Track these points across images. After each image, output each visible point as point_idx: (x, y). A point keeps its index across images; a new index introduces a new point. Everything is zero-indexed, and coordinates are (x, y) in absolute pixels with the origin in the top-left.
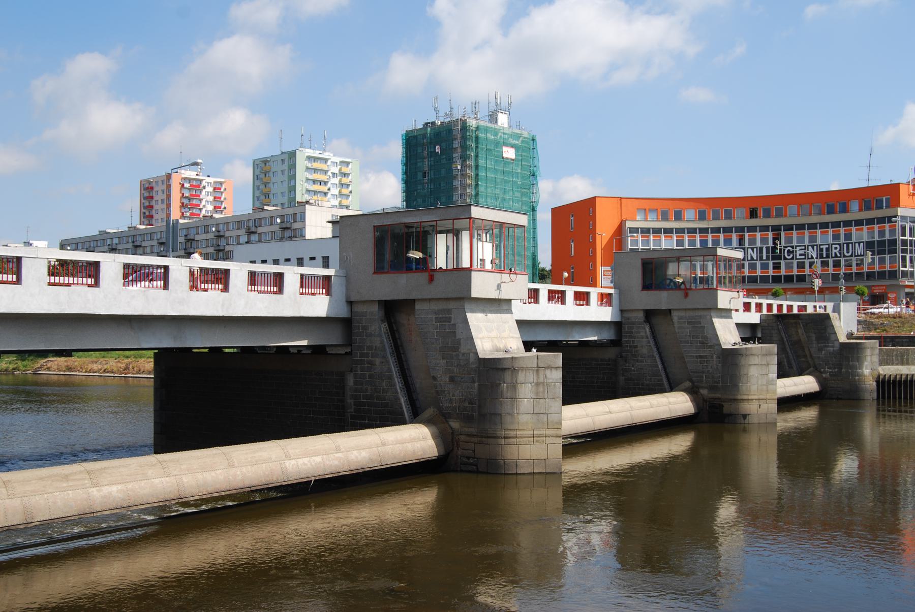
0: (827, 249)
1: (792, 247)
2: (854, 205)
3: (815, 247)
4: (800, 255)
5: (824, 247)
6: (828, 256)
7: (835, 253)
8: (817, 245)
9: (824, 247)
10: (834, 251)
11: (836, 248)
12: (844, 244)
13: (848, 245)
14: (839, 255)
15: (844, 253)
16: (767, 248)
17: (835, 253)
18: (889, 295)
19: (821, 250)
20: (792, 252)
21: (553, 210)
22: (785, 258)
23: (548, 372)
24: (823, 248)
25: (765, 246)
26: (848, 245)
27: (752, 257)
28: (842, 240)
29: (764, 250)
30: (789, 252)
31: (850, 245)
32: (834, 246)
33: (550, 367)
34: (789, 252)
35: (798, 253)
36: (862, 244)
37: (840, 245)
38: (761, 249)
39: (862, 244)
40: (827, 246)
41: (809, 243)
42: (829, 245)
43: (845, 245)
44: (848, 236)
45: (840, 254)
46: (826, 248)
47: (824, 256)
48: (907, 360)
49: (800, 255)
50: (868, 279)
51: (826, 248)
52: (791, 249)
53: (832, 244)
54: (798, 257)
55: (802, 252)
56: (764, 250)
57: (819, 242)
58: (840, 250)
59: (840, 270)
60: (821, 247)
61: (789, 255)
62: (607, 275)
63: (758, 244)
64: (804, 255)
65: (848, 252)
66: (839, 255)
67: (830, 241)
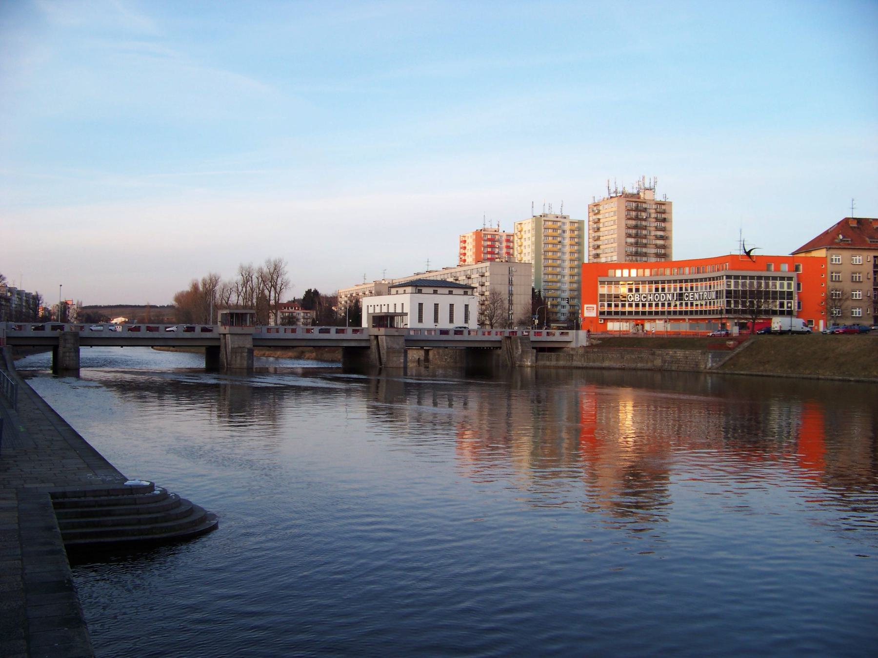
1: (688, 293)
2: (709, 268)
4: (692, 298)
5: (701, 293)
16: (677, 293)
19: (700, 295)
22: (685, 300)
23: (243, 354)
25: (675, 292)
27: (669, 299)
29: (675, 295)
33: (243, 352)
34: (687, 296)
35: (691, 296)
38: (673, 294)
48: (551, 359)
54: (691, 299)
55: (692, 296)
56: (675, 295)
63: (672, 291)
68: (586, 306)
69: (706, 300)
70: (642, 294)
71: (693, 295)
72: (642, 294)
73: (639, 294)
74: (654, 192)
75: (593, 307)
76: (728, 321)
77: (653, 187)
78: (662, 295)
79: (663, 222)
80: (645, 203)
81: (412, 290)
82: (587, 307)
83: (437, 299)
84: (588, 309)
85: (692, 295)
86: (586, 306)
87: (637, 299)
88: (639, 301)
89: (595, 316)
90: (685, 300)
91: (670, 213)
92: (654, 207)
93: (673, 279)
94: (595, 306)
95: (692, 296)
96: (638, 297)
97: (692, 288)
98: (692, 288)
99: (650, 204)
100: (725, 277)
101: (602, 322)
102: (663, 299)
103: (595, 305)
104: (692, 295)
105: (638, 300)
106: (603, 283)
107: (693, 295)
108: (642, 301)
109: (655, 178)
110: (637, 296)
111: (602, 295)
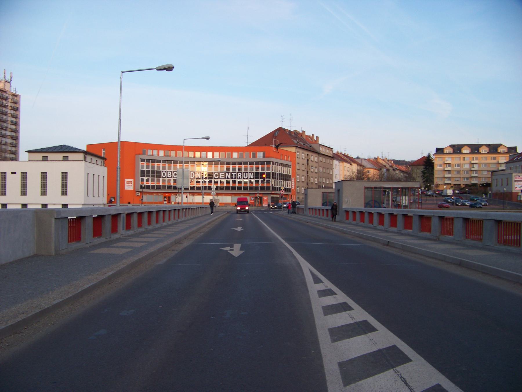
0: (235, 175)
3: (229, 173)
4: (222, 177)
5: (234, 174)
6: (235, 178)
7: (239, 177)
8: (230, 173)
9: (234, 174)
10: (239, 176)
11: (240, 174)
12: (244, 173)
13: (246, 173)
14: (241, 178)
15: (243, 177)
17: (239, 177)
18: (264, 198)
19: (232, 175)
20: (218, 175)
21: (87, 145)
24: (233, 174)
26: (246, 173)
28: (243, 171)
30: (216, 175)
31: (247, 173)
32: (238, 174)
34: (216, 175)
35: (221, 175)
36: (252, 173)
37: (242, 173)
39: (252, 173)
40: (235, 173)
41: (232, 171)
42: (236, 173)
43: (244, 173)
44: (246, 169)
45: (242, 177)
46: (235, 174)
47: (234, 178)
49: (222, 177)
50: (273, 190)
51: (235, 174)
52: (217, 174)
53: (238, 173)
55: (223, 175)
57: (231, 171)
58: (242, 175)
59: (258, 185)
60: (232, 173)
61: (216, 177)
62: (128, 184)
64: (224, 177)
65: (246, 177)
66: (241, 178)
67: (237, 171)
68: (126, 180)
69: (239, 178)
70: (174, 172)
71: (224, 174)
72: (174, 172)
73: (171, 172)
74: (11, 84)
75: (131, 181)
76: (263, 196)
77: (10, 80)
78: (191, 173)
79: (16, 111)
80: (6, 92)
81: (29, 156)
82: (127, 181)
83: (65, 167)
84: (128, 182)
85: (222, 174)
86: (126, 180)
87: (169, 176)
88: (171, 177)
89: (133, 189)
90: (162, 177)
91: (20, 104)
92: (10, 97)
93: (238, 161)
94: (132, 180)
95: (223, 175)
96: (170, 174)
97: (239, 169)
98: (239, 169)
99: (8, 94)
100: (271, 163)
101: (139, 195)
102: (192, 176)
103: (133, 180)
104: (222, 174)
105: (170, 177)
106: (143, 160)
107: (224, 174)
108: (173, 177)
109: (11, 73)
110: (169, 173)
111: (143, 172)
